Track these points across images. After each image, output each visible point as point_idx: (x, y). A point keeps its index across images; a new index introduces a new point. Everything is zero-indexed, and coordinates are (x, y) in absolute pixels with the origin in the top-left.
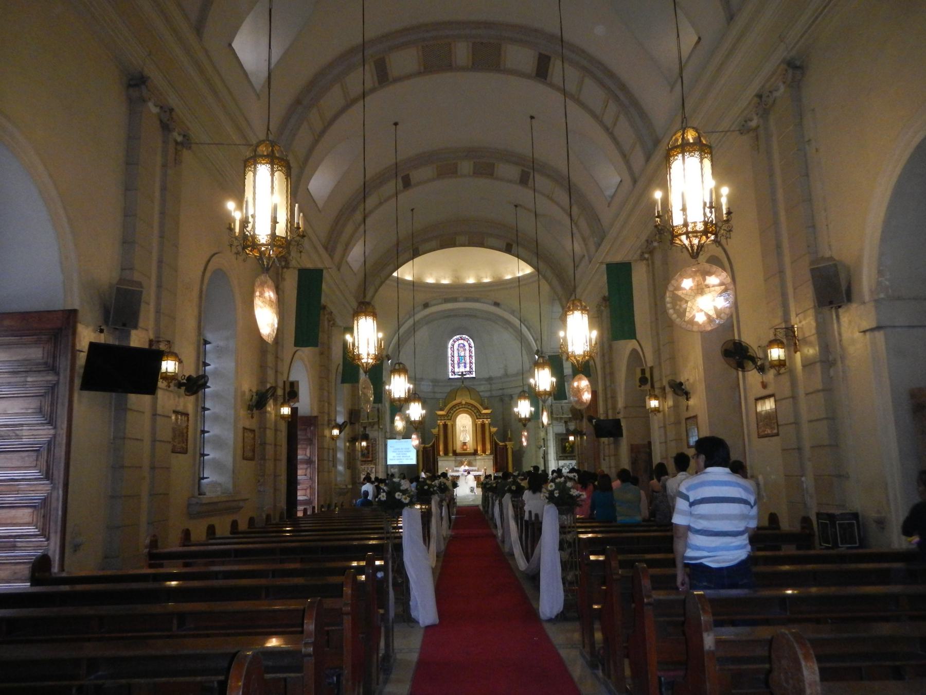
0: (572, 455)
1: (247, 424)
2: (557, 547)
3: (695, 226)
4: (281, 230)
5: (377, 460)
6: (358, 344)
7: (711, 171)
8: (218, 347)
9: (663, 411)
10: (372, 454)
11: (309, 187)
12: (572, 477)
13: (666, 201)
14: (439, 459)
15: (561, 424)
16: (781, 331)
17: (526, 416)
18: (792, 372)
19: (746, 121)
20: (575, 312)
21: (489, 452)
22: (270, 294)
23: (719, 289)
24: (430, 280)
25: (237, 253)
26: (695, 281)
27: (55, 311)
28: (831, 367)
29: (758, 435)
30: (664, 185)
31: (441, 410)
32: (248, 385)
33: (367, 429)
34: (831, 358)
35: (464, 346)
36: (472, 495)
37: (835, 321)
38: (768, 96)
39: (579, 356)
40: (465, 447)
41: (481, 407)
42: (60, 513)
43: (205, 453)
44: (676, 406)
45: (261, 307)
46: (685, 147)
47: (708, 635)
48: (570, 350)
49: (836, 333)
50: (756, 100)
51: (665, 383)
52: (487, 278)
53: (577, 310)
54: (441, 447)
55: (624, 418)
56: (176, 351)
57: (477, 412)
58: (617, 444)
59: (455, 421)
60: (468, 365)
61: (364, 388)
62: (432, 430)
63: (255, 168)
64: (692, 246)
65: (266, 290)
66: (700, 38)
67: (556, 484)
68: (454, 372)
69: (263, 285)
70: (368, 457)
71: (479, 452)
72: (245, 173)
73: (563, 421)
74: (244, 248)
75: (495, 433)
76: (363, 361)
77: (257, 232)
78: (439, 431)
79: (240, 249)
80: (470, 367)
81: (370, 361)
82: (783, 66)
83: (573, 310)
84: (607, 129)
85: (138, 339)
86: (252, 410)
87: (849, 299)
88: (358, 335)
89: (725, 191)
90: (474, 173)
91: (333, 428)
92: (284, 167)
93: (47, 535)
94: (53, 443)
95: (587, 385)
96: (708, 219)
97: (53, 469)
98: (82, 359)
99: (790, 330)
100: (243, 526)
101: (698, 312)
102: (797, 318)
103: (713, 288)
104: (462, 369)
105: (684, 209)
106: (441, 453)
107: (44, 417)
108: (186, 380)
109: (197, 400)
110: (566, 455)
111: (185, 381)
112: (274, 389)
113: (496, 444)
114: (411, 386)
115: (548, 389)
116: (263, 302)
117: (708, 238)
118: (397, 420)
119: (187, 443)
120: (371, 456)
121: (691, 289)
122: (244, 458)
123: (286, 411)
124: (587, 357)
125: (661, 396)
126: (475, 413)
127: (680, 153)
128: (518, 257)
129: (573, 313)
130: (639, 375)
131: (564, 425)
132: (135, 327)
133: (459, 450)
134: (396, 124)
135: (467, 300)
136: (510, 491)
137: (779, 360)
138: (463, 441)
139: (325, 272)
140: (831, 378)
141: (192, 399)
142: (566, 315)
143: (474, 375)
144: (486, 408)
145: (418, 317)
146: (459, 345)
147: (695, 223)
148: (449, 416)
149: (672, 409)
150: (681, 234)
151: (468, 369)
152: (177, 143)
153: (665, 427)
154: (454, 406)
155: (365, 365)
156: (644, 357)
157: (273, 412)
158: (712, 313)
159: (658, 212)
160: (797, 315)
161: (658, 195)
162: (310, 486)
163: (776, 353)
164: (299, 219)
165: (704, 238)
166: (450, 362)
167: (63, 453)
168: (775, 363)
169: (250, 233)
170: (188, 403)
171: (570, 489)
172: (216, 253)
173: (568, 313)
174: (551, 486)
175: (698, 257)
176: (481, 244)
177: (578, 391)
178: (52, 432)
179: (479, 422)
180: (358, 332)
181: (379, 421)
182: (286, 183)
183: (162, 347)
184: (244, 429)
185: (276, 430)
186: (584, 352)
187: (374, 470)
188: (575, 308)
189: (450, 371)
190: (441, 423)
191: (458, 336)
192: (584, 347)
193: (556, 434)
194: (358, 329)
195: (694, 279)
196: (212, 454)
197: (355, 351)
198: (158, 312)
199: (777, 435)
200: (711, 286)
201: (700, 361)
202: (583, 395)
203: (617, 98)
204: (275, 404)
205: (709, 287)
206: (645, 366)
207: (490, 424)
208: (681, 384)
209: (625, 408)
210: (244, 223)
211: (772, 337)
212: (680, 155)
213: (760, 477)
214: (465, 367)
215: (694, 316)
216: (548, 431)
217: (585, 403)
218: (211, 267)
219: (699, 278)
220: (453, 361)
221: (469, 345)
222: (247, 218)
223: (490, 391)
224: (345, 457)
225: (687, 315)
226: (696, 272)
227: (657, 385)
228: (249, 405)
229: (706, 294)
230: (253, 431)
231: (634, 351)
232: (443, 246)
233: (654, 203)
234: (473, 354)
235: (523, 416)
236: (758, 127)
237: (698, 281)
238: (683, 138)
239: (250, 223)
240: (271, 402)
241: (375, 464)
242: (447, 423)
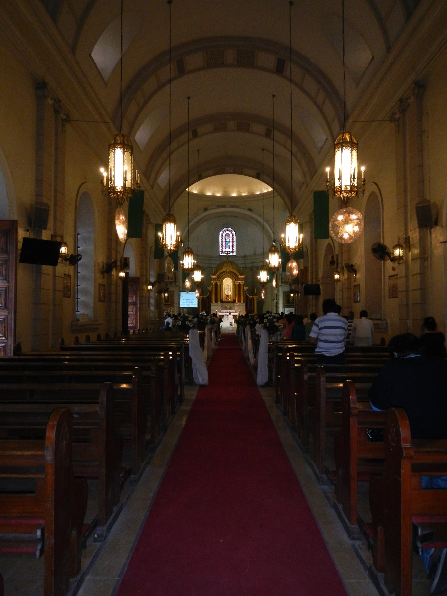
1: (101, 281)
2: (267, 351)
4: (128, 184)
5: (174, 305)
6: (166, 238)
8: (84, 237)
9: (342, 281)
10: (171, 301)
11: (135, 138)
12: (277, 316)
13: (332, 173)
14: (212, 305)
15: (287, 286)
16: (402, 239)
17: (264, 281)
18: (406, 263)
19: (393, 114)
20: (291, 223)
21: (243, 301)
22: (122, 218)
24: (209, 194)
25: (105, 195)
26: (345, 217)
27: (6, 220)
28: (425, 261)
29: (389, 297)
30: (332, 163)
31: (214, 275)
32: (101, 259)
33: (168, 286)
34: (426, 256)
35: (229, 235)
36: (231, 327)
37: (429, 236)
38: (405, 102)
39: (292, 249)
40: (228, 298)
41: (238, 274)
42: (13, 326)
43: (78, 297)
44: (349, 278)
45: (119, 225)
46: (343, 144)
48: (287, 245)
49: (429, 242)
51: (344, 265)
52: (244, 193)
54: (213, 298)
56: (65, 241)
57: (236, 277)
58: (317, 299)
59: (222, 282)
60: (231, 247)
61: (169, 264)
62: (208, 287)
63: (115, 150)
65: (121, 215)
66: (373, 58)
67: (268, 320)
68: (222, 251)
69: (119, 213)
70: (169, 302)
71: (236, 302)
72: (109, 152)
73: (288, 284)
74: (109, 193)
75: (247, 290)
76: (168, 248)
77: (116, 185)
78: (212, 287)
79: (107, 193)
80: (233, 248)
81: (172, 248)
83: (290, 222)
84: (318, 106)
85: (46, 235)
86: (103, 274)
87: (436, 223)
88: (165, 233)
91: (149, 285)
92: (130, 150)
93: (7, 337)
94: (7, 290)
95: (296, 266)
96: (353, 184)
97: (8, 304)
98: (20, 245)
99: (407, 240)
100: (103, 337)
101: (345, 233)
102: (411, 233)
104: (228, 250)
105: (340, 178)
106: (213, 301)
107: (2, 276)
108: (70, 257)
109: (75, 267)
110: (290, 304)
111: (69, 257)
112: (116, 262)
113: (247, 296)
114: (195, 262)
115: (277, 266)
116: (120, 222)
118: (187, 281)
119: (70, 292)
120: (170, 301)
121: (342, 220)
122: (100, 301)
123: (122, 274)
124: (296, 250)
126: (235, 278)
127: (341, 147)
128: (263, 181)
129: (290, 224)
131: (289, 286)
132: (46, 229)
133: (224, 299)
134: (189, 98)
135: (232, 206)
136: (249, 324)
138: (226, 295)
139: (146, 193)
140: (425, 267)
141: (72, 267)
142: (286, 225)
143: (235, 254)
144: (241, 275)
145: (200, 216)
146: (226, 234)
147: (346, 186)
148: (218, 279)
149: (347, 280)
151: (231, 250)
152: (63, 120)
153: (342, 290)
154: (222, 273)
155: (169, 250)
156: (334, 248)
157: (115, 275)
158: (352, 234)
161: (328, 169)
162: (135, 318)
163: (398, 252)
164: (137, 178)
166: (220, 245)
167: (13, 296)
168: (397, 257)
169: (112, 186)
170: (70, 270)
171: (274, 322)
172: (83, 183)
173: (287, 224)
174: (265, 321)
175: (347, 204)
176: (241, 173)
177: (291, 269)
178: (7, 284)
179: (237, 283)
180: (165, 231)
181: (175, 281)
182: (131, 158)
183: (58, 239)
184: (99, 284)
185: (117, 286)
186: (295, 246)
187: (172, 310)
189: (220, 250)
190: (213, 283)
191: (225, 229)
192: (295, 244)
193: (284, 292)
194: (165, 230)
196: (82, 298)
197: (164, 242)
198: (55, 218)
199: (397, 297)
201: (363, 253)
202: (294, 271)
204: (116, 271)
205: (351, 220)
206: (334, 254)
207: (244, 285)
208: (352, 266)
209: (323, 278)
210: (109, 179)
211: (397, 243)
212: (341, 148)
213: (388, 320)
214: (230, 248)
215: (343, 235)
216: (279, 290)
217: (294, 276)
218: (81, 192)
219: (347, 215)
220: (222, 245)
221: (233, 234)
222: (111, 177)
223: (245, 264)
224: (155, 302)
226: (345, 212)
227: (340, 266)
228: (102, 271)
229: (349, 224)
230: (104, 286)
231: (329, 244)
232: (217, 173)
233: (325, 174)
234: (235, 241)
235: (262, 281)
236: (399, 118)
237: (346, 217)
239: (112, 180)
240: (114, 270)
241: (173, 307)
242: (217, 283)
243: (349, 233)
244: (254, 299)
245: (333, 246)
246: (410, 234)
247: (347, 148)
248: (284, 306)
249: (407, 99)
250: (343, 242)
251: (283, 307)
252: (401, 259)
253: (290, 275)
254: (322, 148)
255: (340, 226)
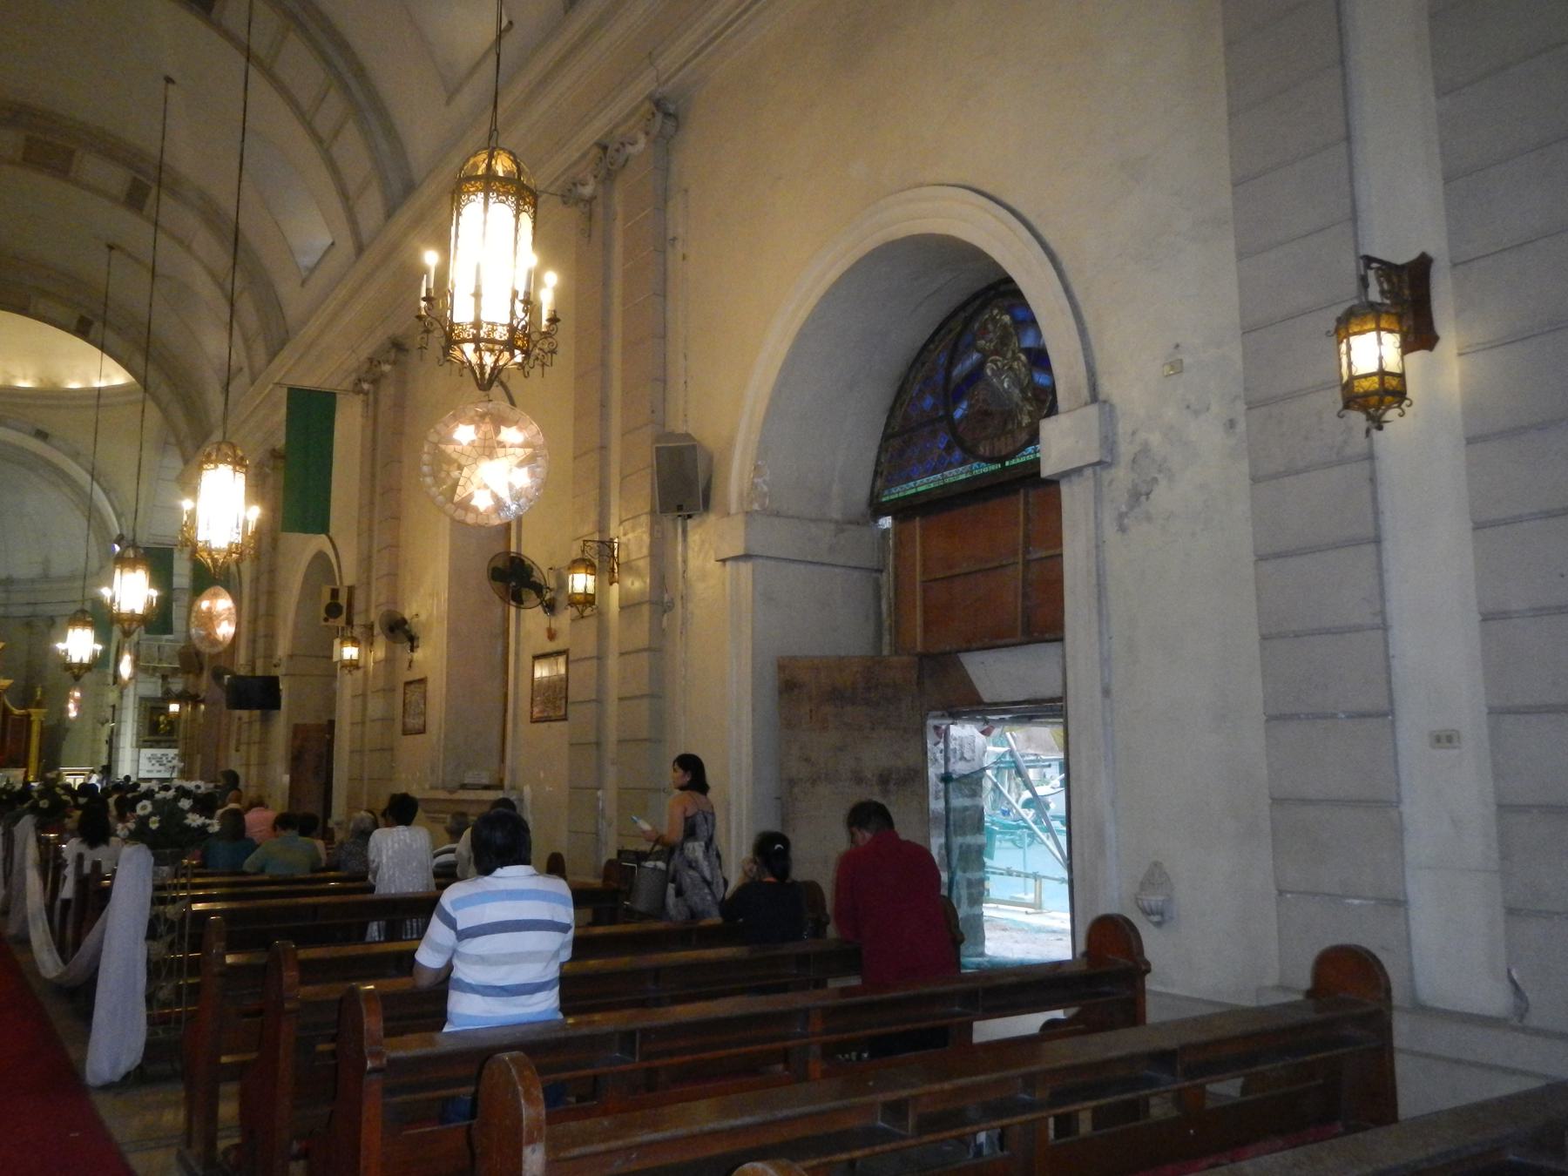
0: (170, 738)
3: (493, 330)
7: (531, 238)
9: (365, 667)
12: (193, 788)
15: (153, 679)
17: (82, 660)
18: (601, 615)
19: (575, 184)
23: (520, 452)
28: (665, 612)
29: (532, 717)
30: (443, 241)
37: (680, 538)
39: (219, 551)
44: (389, 661)
46: (489, 182)
47: (534, 1151)
49: (680, 559)
50: (595, 151)
53: (224, 461)
55: (286, 675)
58: (266, 721)
64: (482, 366)
67: (155, 803)
82: (648, 105)
83: (217, 462)
89: (551, 279)
90: (24, 159)
95: (229, 609)
99: (606, 546)
101: (479, 488)
102: (621, 528)
103: (512, 450)
105: (477, 295)
117: (513, 356)
121: (472, 444)
124: (234, 555)
125: (365, 639)
127: (481, 191)
128: (103, 348)
129: (216, 467)
130: (326, 598)
131: (160, 681)
137: (586, 594)
140: (664, 630)
147: (493, 324)
149: (383, 663)
150: (465, 341)
153: (364, 695)
156: (339, 567)
158: (505, 495)
159: (428, 290)
160: (621, 523)
161: (431, 258)
163: (581, 582)
165: (507, 355)
168: (578, 597)
173: (205, 466)
174: (144, 808)
175: (489, 389)
177: (210, 619)
186: (231, 544)
188: (222, 459)
195: (478, 428)
199: (565, 718)
200: (508, 445)
202: (219, 626)
203: (345, 89)
205: (504, 447)
206: (338, 583)
208: (404, 621)
209: (291, 657)
212: (481, 195)
213: (527, 789)
215: (471, 496)
217: (220, 643)
219: (487, 427)
225: (457, 491)
226: (483, 416)
227: (358, 620)
229: (498, 458)
231: (320, 556)
233: (419, 272)
235: (76, 660)
236: (593, 198)
237: (485, 433)
238: (489, 166)
243: (496, 490)
244: (32, 719)
245: (334, 560)
246: (615, 531)
247: (504, 198)
248: (141, 743)
249: (623, 144)
250: (470, 519)
251: (134, 745)
252: (588, 602)
253: (203, 639)
254: (312, 270)
255: (463, 461)
